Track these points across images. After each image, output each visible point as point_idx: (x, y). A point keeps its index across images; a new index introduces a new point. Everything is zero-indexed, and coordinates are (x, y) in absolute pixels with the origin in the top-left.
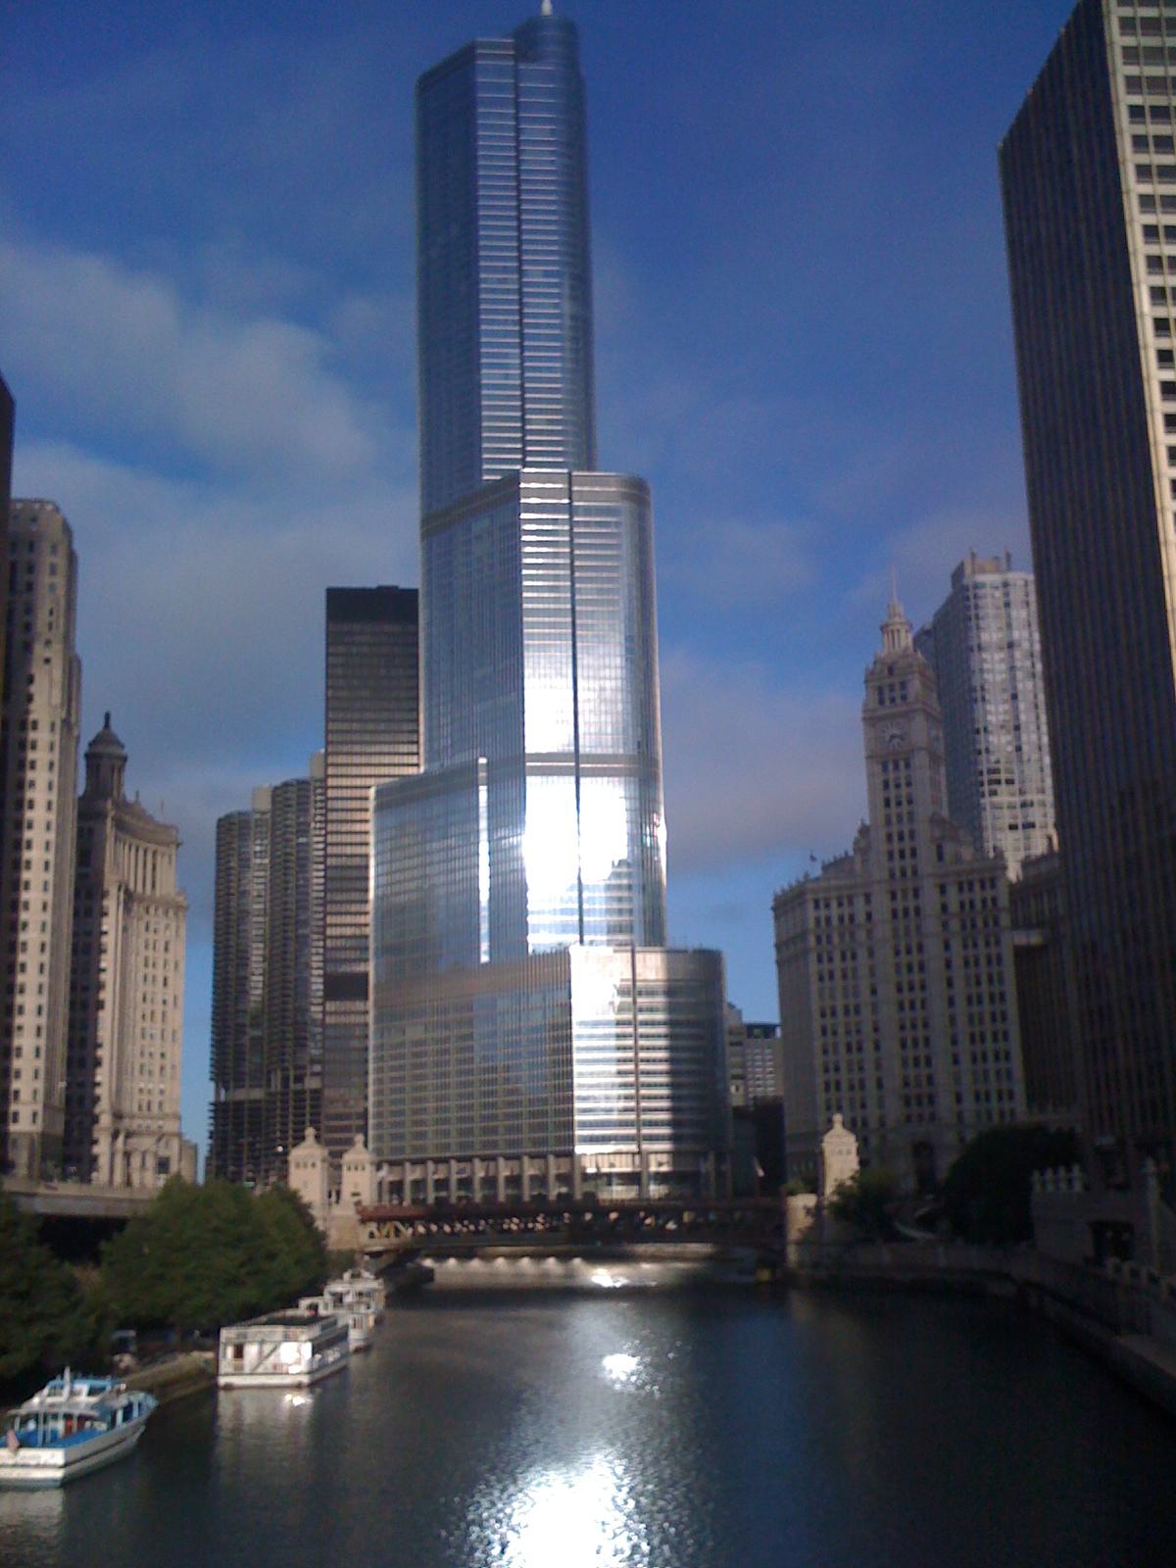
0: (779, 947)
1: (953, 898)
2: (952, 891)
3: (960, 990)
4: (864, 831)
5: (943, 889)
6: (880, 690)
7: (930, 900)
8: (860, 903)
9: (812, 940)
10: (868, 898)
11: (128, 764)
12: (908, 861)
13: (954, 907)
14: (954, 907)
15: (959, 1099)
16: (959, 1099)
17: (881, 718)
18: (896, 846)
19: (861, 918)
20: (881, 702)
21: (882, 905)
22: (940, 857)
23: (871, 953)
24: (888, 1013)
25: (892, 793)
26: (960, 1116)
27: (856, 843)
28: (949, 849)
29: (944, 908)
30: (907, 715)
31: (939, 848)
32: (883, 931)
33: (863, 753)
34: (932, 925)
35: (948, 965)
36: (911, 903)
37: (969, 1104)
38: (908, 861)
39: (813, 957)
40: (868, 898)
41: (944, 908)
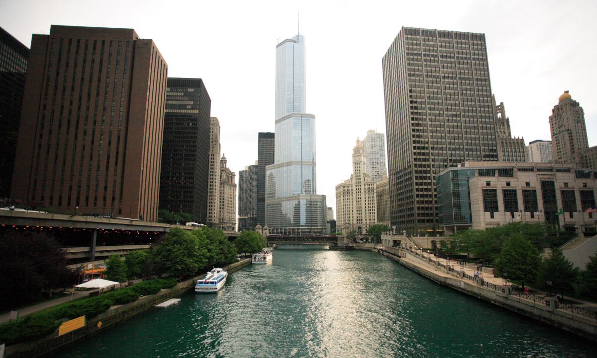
0: (336, 194)
1: (366, 187)
2: (366, 185)
3: (367, 202)
4: (352, 175)
5: (365, 185)
7: (363, 187)
8: (350, 187)
9: (342, 194)
10: (352, 186)
11: (227, 162)
12: (359, 181)
13: (366, 188)
14: (366, 188)
15: (366, 220)
16: (366, 220)
18: (357, 178)
19: (350, 190)
21: (354, 188)
24: (355, 205)
25: (357, 169)
26: (366, 223)
28: (366, 178)
29: (365, 188)
30: (360, 156)
33: (352, 162)
34: (363, 191)
35: (365, 198)
36: (359, 188)
37: (368, 221)
38: (359, 181)
39: (342, 196)
41: (365, 188)
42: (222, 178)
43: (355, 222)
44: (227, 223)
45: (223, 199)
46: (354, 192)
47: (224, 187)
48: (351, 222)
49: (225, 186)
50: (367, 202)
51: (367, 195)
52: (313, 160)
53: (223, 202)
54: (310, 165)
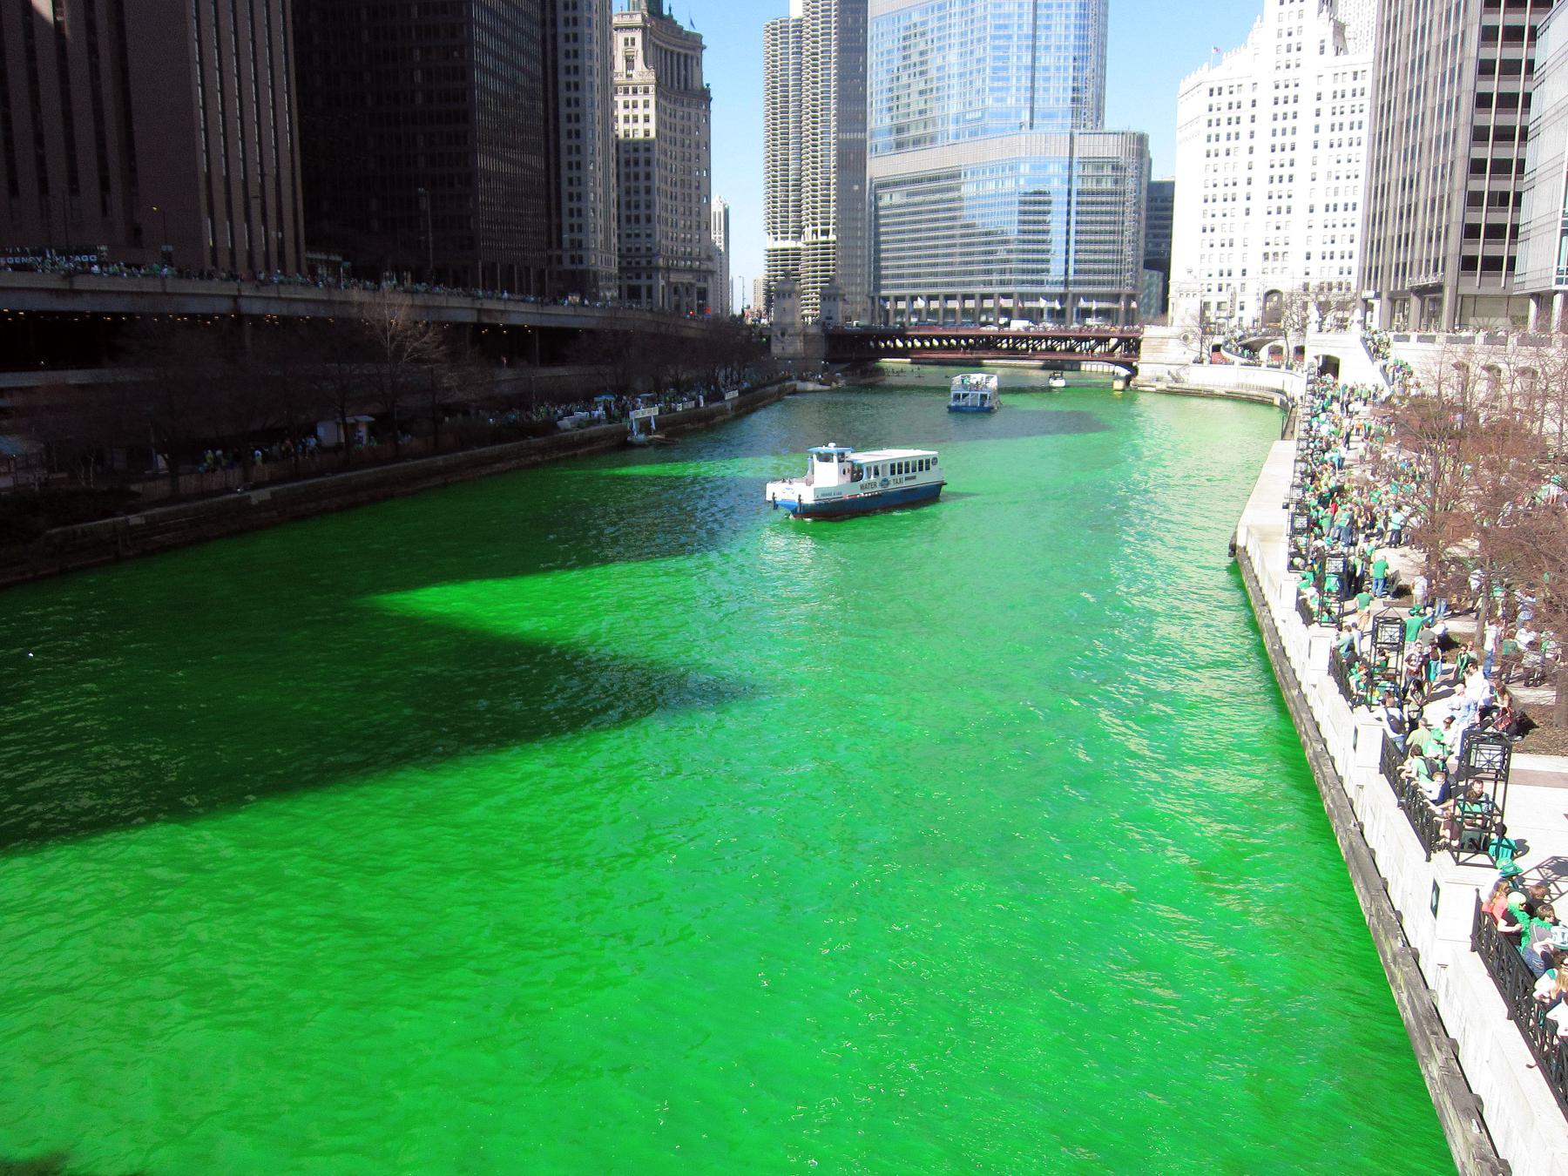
44: (668, 269)
45: (648, 163)
53: (648, 176)
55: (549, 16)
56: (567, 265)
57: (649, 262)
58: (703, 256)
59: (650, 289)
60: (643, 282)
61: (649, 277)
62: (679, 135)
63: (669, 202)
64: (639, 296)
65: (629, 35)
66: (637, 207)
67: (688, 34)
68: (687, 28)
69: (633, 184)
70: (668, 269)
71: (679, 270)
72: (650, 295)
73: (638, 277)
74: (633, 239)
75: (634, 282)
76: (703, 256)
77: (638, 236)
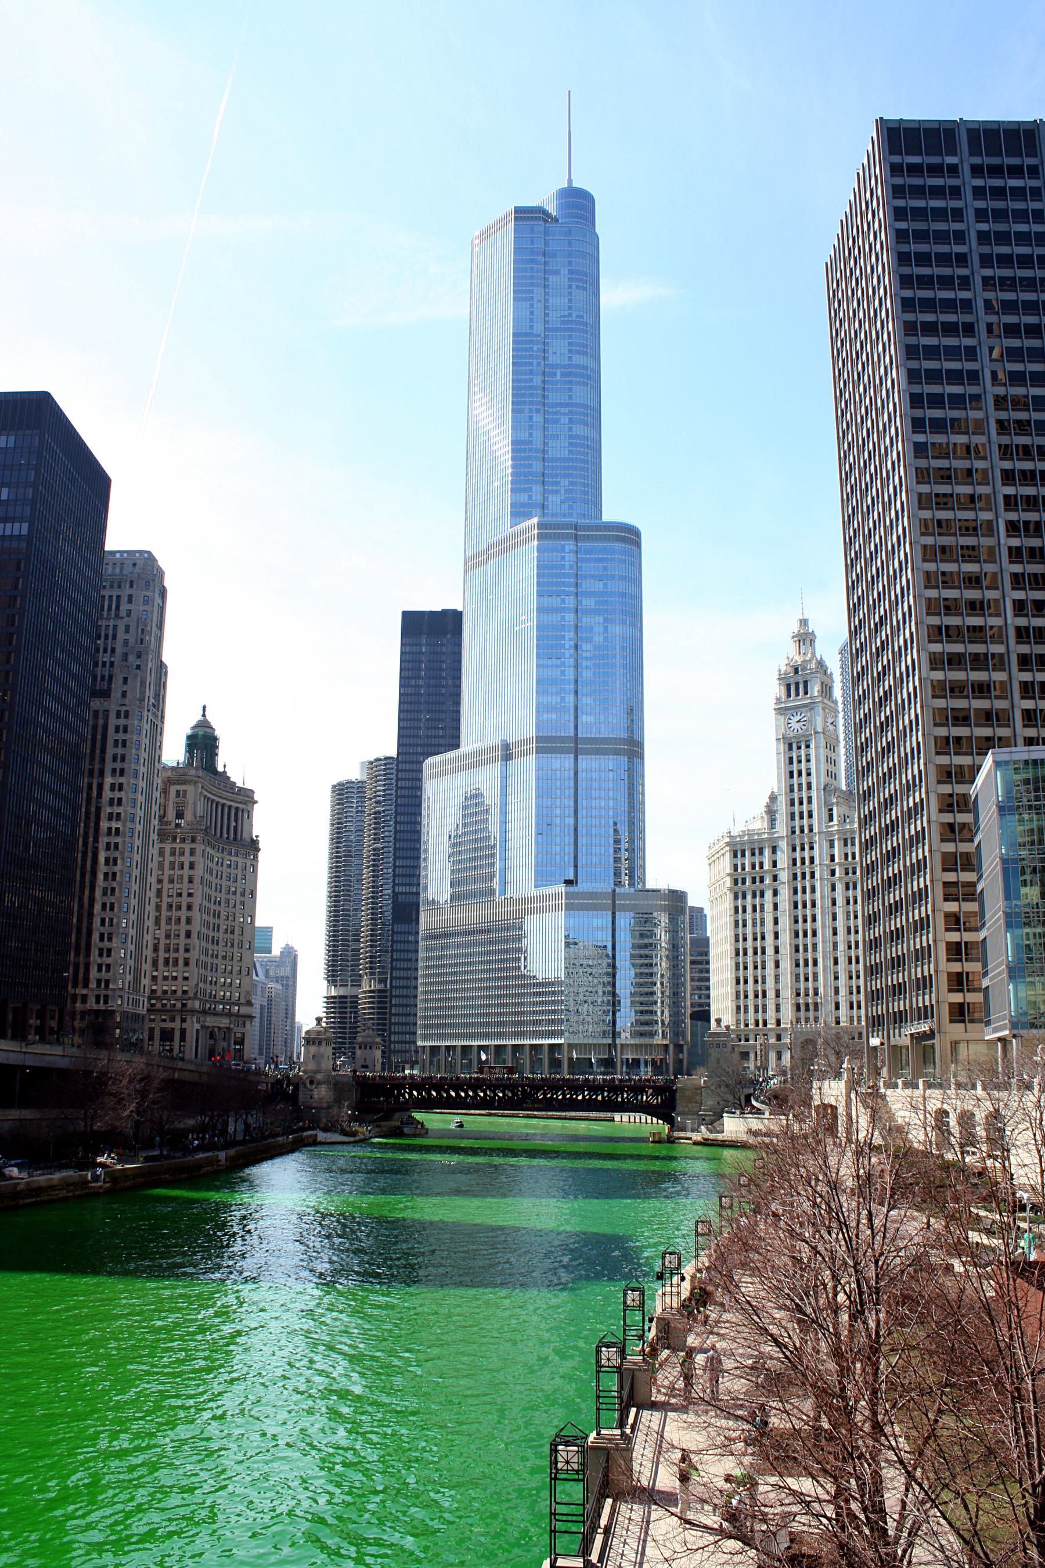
3: (840, 923)
4: (773, 798)
6: (788, 687)
8: (767, 852)
10: (774, 850)
17: (786, 709)
20: (789, 695)
22: (831, 819)
23: (775, 893)
25: (795, 767)
27: (768, 806)
31: (831, 810)
32: (784, 876)
40: (774, 850)
42: (189, 815)
43: (787, 1014)
44: (204, 1012)
46: (784, 876)
47: (192, 852)
48: (771, 1015)
49: (199, 847)
50: (840, 923)
51: (840, 887)
52: (631, 729)
54: (617, 752)
55: (97, 766)
56: (91, 1004)
57: (184, 1005)
58: (243, 1000)
59: (183, 1032)
60: (177, 1025)
61: (183, 1020)
62: (224, 883)
63: (210, 946)
64: (172, 1040)
65: (181, 788)
66: (177, 950)
67: (240, 789)
68: (239, 784)
69: (174, 927)
70: (204, 1012)
71: (216, 1014)
72: (183, 1038)
73: (173, 1020)
74: (170, 982)
75: (168, 1025)
76: (243, 1000)
77: (175, 978)
